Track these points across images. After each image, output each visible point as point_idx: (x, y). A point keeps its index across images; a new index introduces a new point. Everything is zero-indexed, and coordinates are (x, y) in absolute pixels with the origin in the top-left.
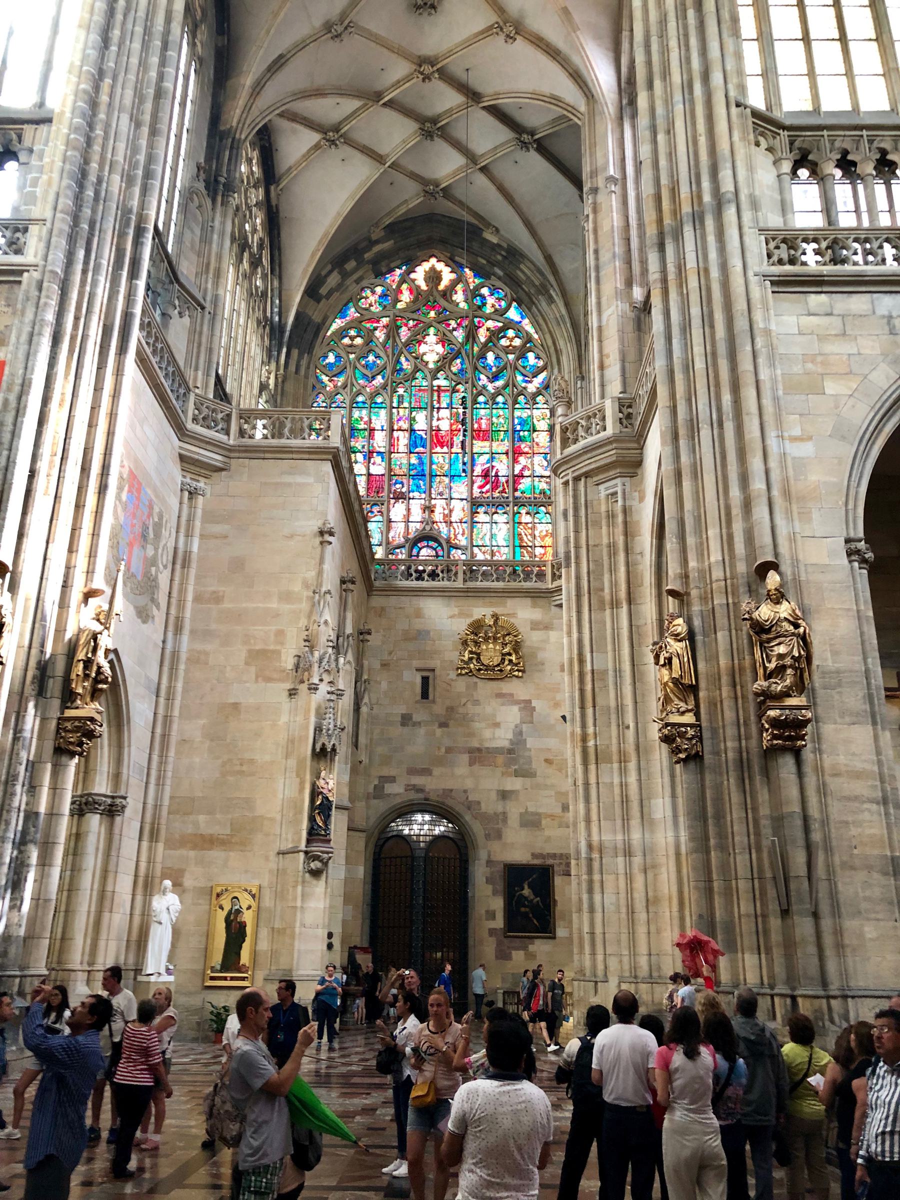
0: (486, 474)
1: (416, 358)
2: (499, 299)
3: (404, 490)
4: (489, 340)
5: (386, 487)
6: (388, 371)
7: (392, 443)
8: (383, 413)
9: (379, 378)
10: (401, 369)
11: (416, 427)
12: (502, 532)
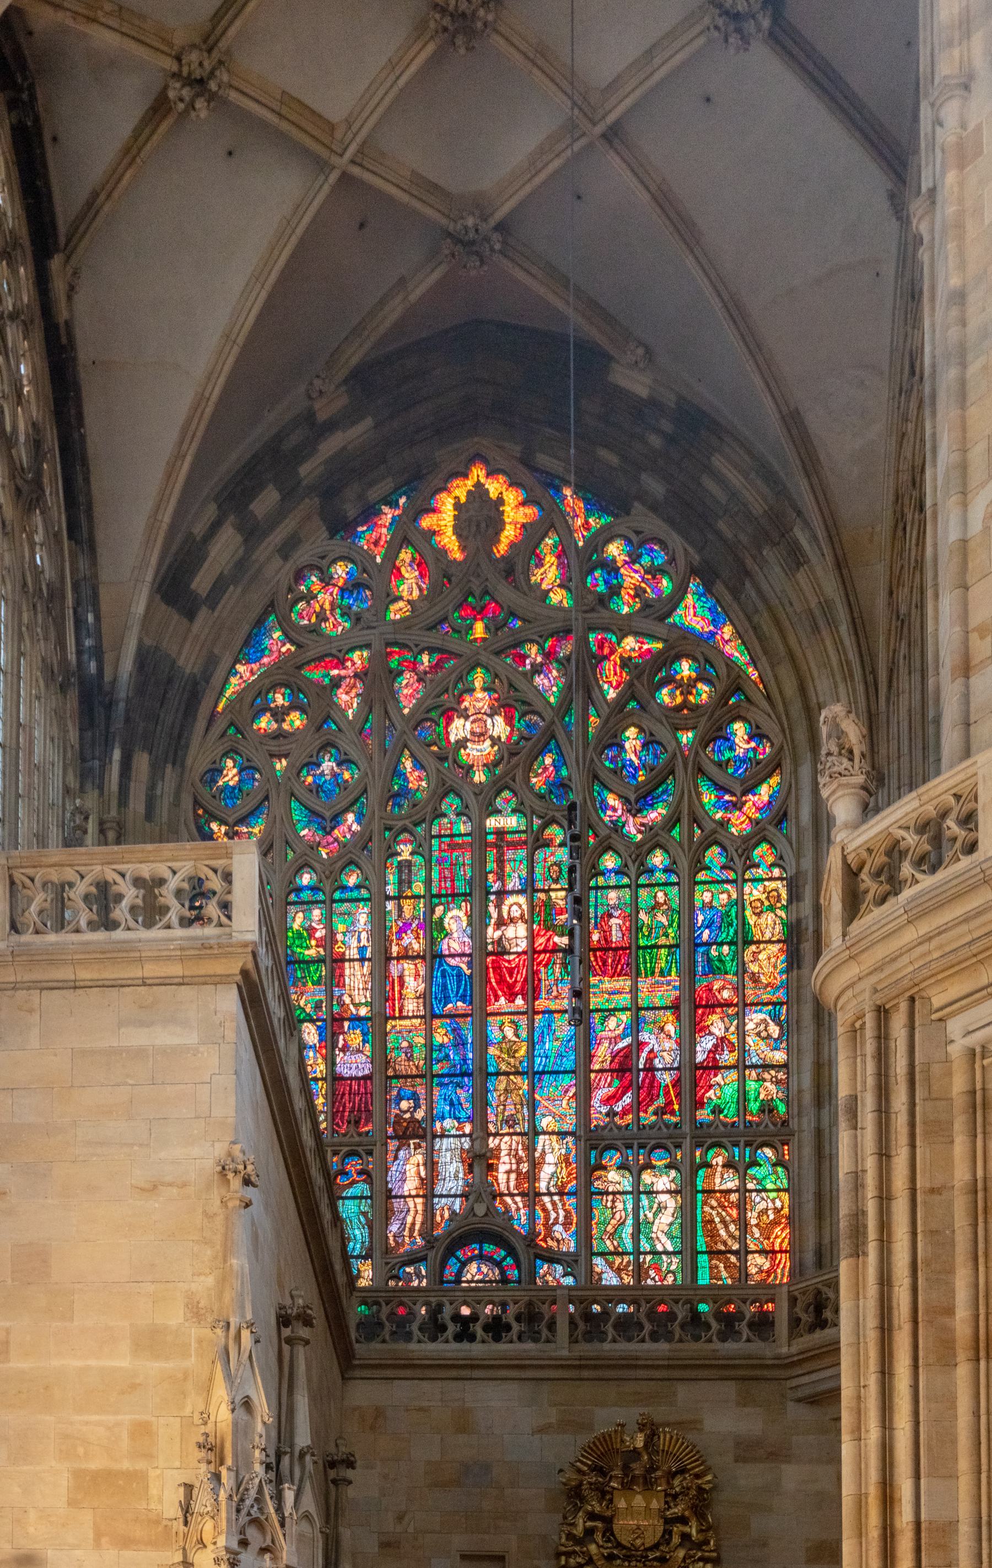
0: (623, 1066)
1: (442, 759)
2: (654, 572)
3: (420, 1114)
4: (629, 693)
6: (374, 795)
8: (363, 917)
9: (351, 817)
10: (405, 792)
11: (446, 946)
12: (663, 1223)
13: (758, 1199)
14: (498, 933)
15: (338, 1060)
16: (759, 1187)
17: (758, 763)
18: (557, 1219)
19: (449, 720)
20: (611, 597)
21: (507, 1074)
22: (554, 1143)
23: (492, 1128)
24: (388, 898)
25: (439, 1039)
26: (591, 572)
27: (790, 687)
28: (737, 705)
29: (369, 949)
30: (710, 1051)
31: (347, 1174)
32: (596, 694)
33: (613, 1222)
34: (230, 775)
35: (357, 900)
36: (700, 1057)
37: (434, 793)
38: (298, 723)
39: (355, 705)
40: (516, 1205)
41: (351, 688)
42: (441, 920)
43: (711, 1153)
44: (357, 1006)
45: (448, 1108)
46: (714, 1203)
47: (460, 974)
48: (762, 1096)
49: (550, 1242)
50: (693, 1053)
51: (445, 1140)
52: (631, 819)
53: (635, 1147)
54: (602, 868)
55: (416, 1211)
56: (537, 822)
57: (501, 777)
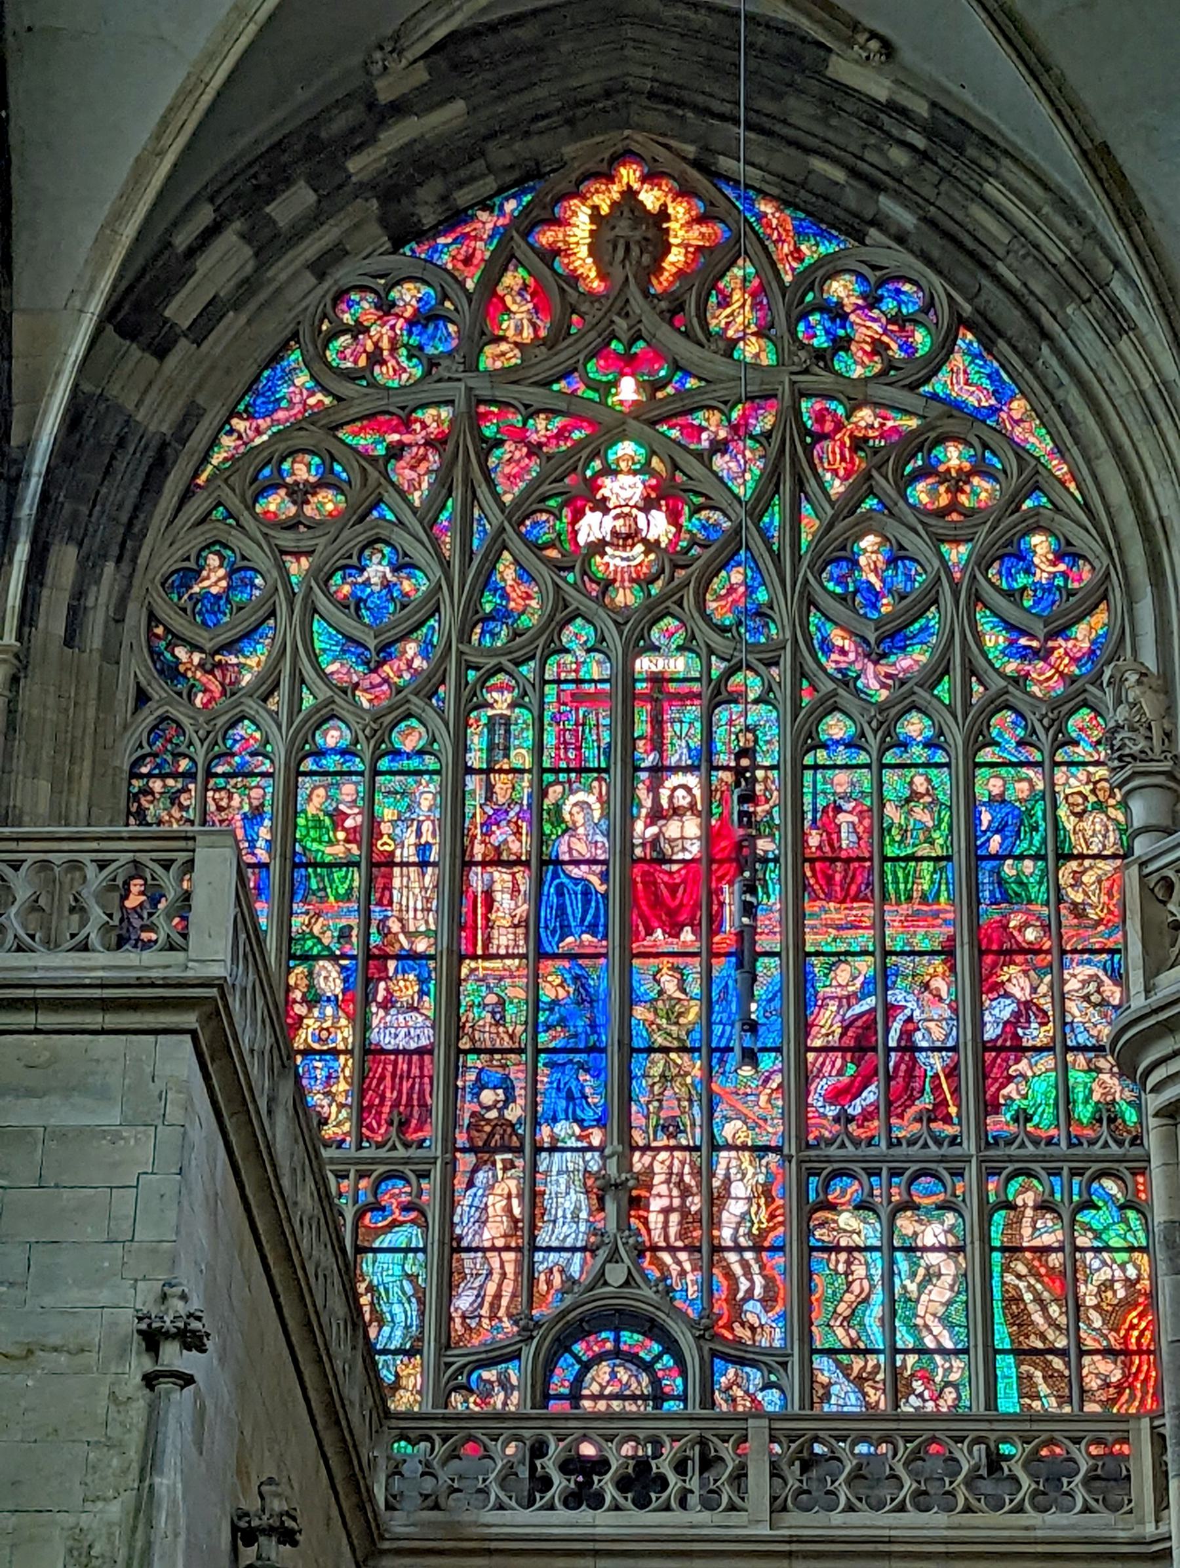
0: (860, 1041)
3: (514, 1113)
4: (864, 486)
5: (437, 1103)
6: (449, 616)
7: (463, 918)
8: (427, 794)
9: (411, 648)
10: (501, 615)
13: (1096, 1264)
14: (653, 830)
15: (375, 1022)
16: (1096, 1244)
17: (1071, 593)
18: (751, 1290)
19: (578, 515)
20: (834, 354)
21: (665, 1050)
22: (746, 1165)
23: (639, 1138)
24: (470, 771)
25: (548, 993)
26: (804, 316)
27: (1117, 491)
28: (1036, 511)
29: (435, 849)
30: (1006, 1023)
31: (383, 1209)
32: (812, 485)
33: (848, 1297)
34: (214, 579)
35: (418, 773)
36: (991, 1032)
37: (551, 618)
38: (330, 507)
39: (425, 485)
40: (681, 1267)
41: (420, 461)
42: (558, 807)
43: (1014, 1186)
44: (411, 935)
45: (563, 1103)
46: (1022, 1269)
47: (587, 893)
48: (1096, 1097)
49: (739, 1330)
50: (979, 1025)
51: (557, 1156)
52: (870, 666)
53: (884, 1173)
54: (824, 737)
55: (504, 1275)
56: (718, 667)
57: (664, 597)
